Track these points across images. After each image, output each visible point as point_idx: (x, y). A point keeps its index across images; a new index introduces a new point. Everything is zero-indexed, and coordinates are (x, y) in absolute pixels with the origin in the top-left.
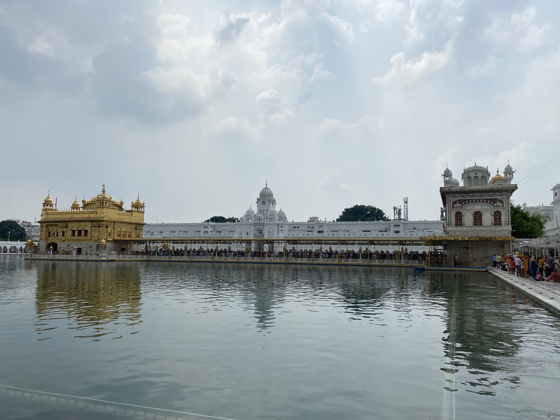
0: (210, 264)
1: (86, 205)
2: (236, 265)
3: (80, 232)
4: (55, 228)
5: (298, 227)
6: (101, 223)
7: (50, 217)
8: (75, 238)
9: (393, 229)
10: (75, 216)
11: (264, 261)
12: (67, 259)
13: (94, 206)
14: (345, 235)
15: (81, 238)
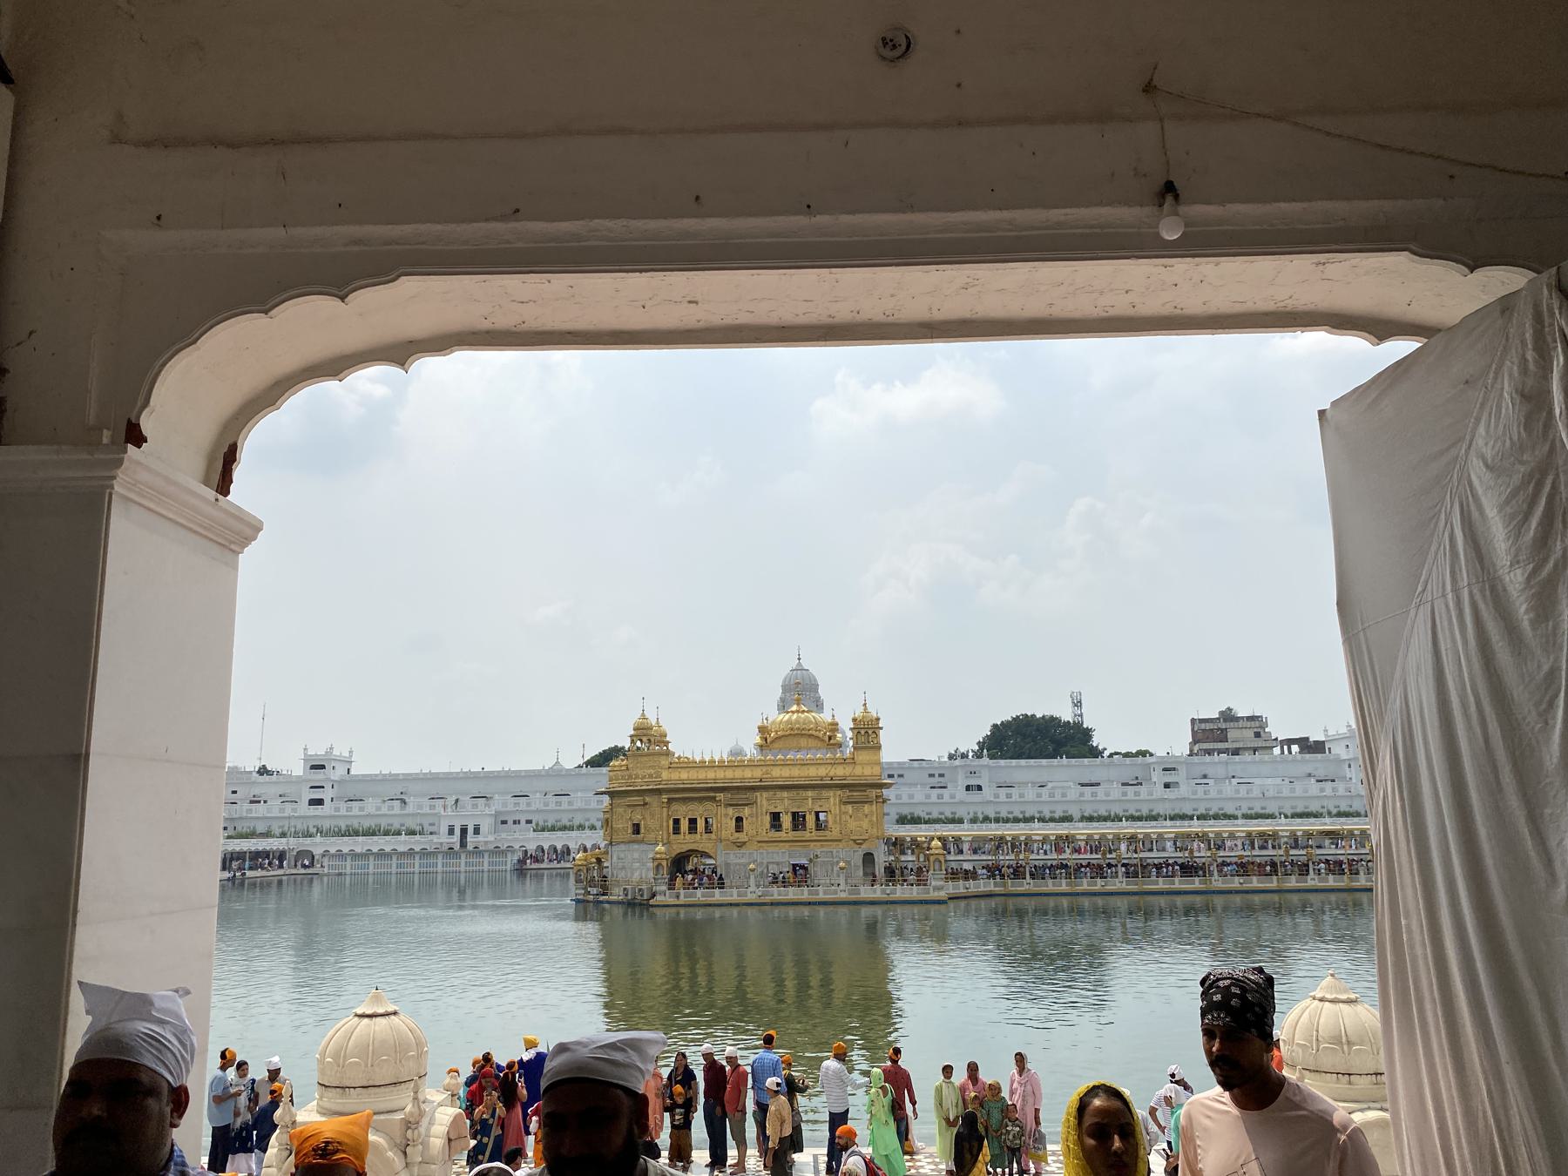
0: (1198, 899)
1: (769, 739)
2: (1276, 897)
3: (798, 821)
4: (698, 811)
5: (901, 776)
6: (873, 793)
7: (684, 775)
8: (782, 835)
9: (1158, 777)
10: (776, 772)
11: (1355, 884)
12: (813, 898)
13: (803, 742)
14: (1039, 795)
15: (807, 835)
